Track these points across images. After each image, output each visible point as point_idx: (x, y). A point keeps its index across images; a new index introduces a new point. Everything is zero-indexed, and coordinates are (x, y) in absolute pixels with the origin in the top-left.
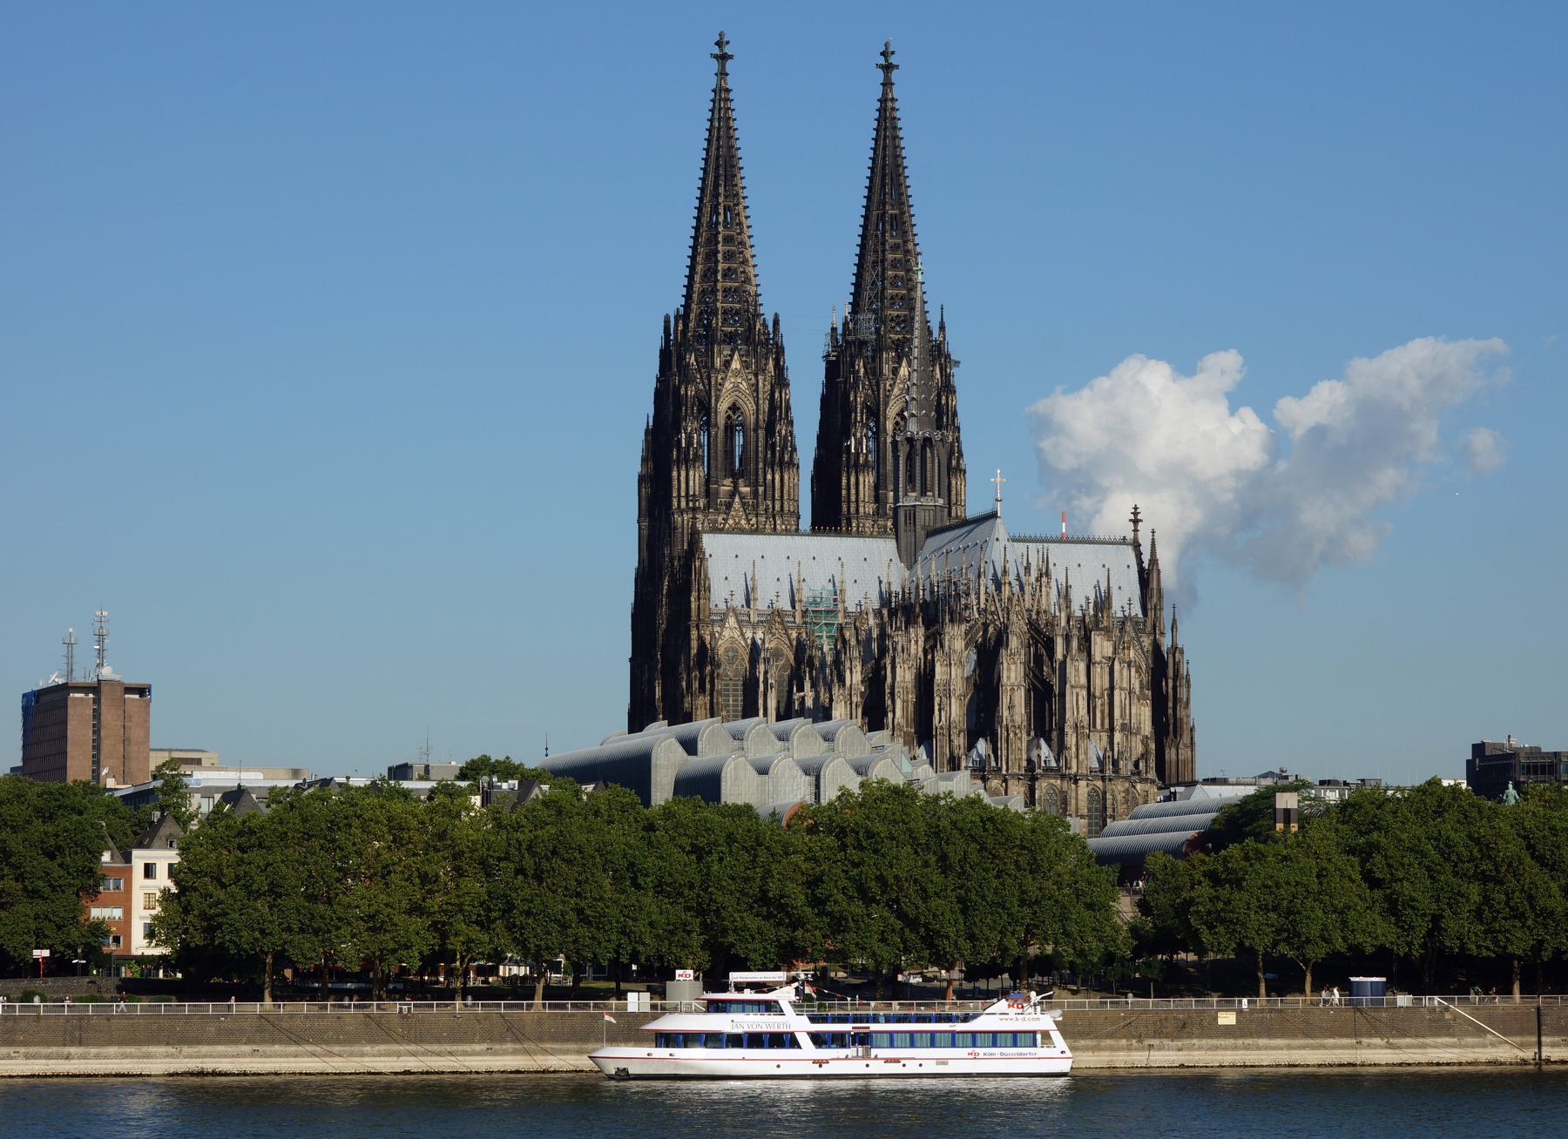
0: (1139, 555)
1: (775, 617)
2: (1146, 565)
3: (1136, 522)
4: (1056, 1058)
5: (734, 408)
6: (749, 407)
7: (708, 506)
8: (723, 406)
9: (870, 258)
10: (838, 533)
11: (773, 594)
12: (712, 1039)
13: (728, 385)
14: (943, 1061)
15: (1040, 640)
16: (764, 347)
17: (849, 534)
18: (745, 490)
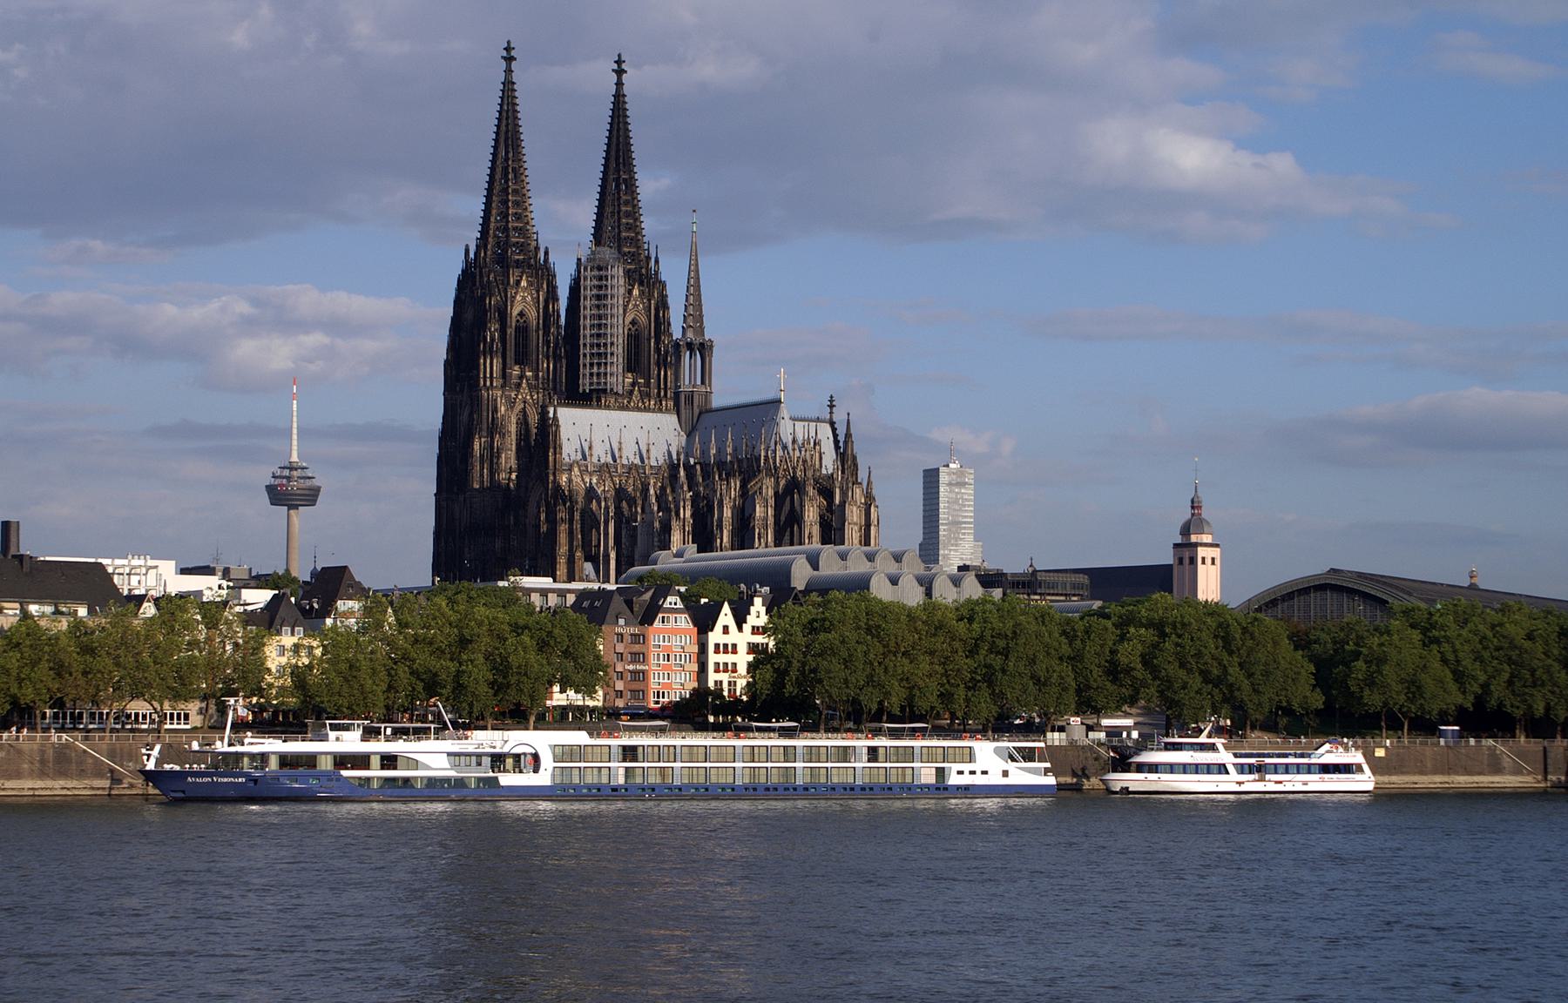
0: (834, 430)
1: (603, 469)
2: (841, 438)
3: (831, 406)
4: (1365, 781)
5: (521, 314)
6: (532, 314)
7: (503, 386)
8: (515, 312)
9: (608, 210)
10: (590, 406)
11: (600, 454)
12: (1172, 768)
13: (519, 298)
14: (1305, 783)
15: (826, 492)
16: (543, 273)
17: (599, 407)
18: (529, 374)
